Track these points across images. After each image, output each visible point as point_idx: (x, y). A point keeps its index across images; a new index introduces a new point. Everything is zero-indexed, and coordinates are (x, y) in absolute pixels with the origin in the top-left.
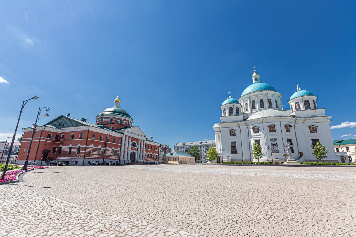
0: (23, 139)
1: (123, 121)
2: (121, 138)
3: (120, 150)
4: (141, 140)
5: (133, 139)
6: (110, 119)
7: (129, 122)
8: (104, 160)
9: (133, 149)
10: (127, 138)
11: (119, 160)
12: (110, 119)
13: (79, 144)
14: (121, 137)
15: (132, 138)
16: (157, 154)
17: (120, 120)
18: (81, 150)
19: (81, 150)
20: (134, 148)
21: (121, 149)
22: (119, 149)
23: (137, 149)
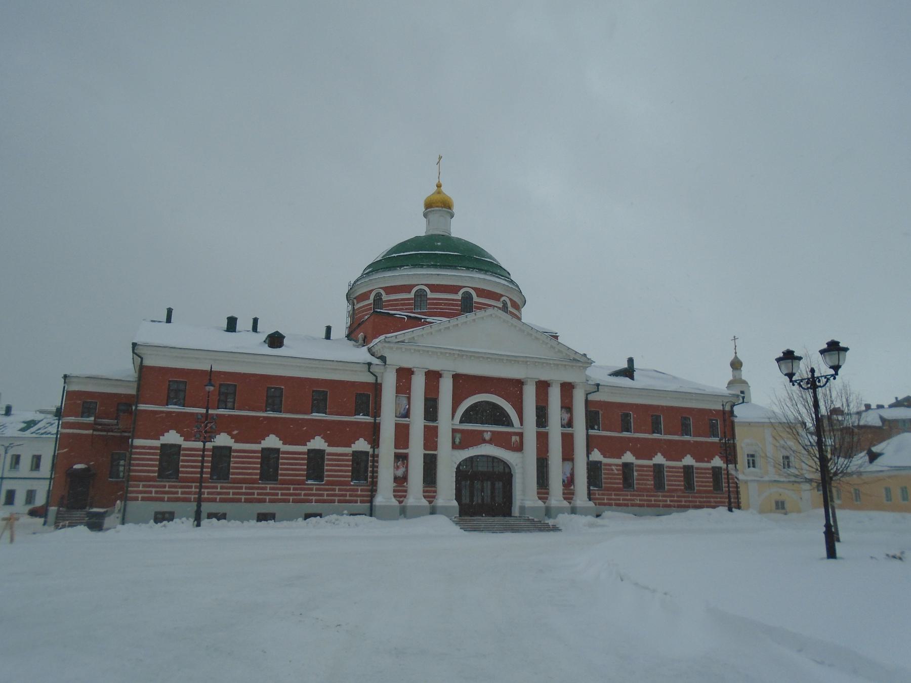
0: (130, 434)
1: (430, 295)
2: (377, 388)
3: (371, 451)
4: (543, 387)
5: (465, 384)
6: (372, 297)
7: (467, 298)
8: (199, 506)
9: (484, 441)
10: (418, 384)
11: (371, 502)
12: (372, 297)
13: (362, 440)
14: (371, 379)
15: (456, 377)
16: (717, 462)
17: (412, 295)
18: (257, 458)
19: (257, 458)
20: (487, 436)
21: (375, 442)
22: (361, 445)
23: (514, 438)
